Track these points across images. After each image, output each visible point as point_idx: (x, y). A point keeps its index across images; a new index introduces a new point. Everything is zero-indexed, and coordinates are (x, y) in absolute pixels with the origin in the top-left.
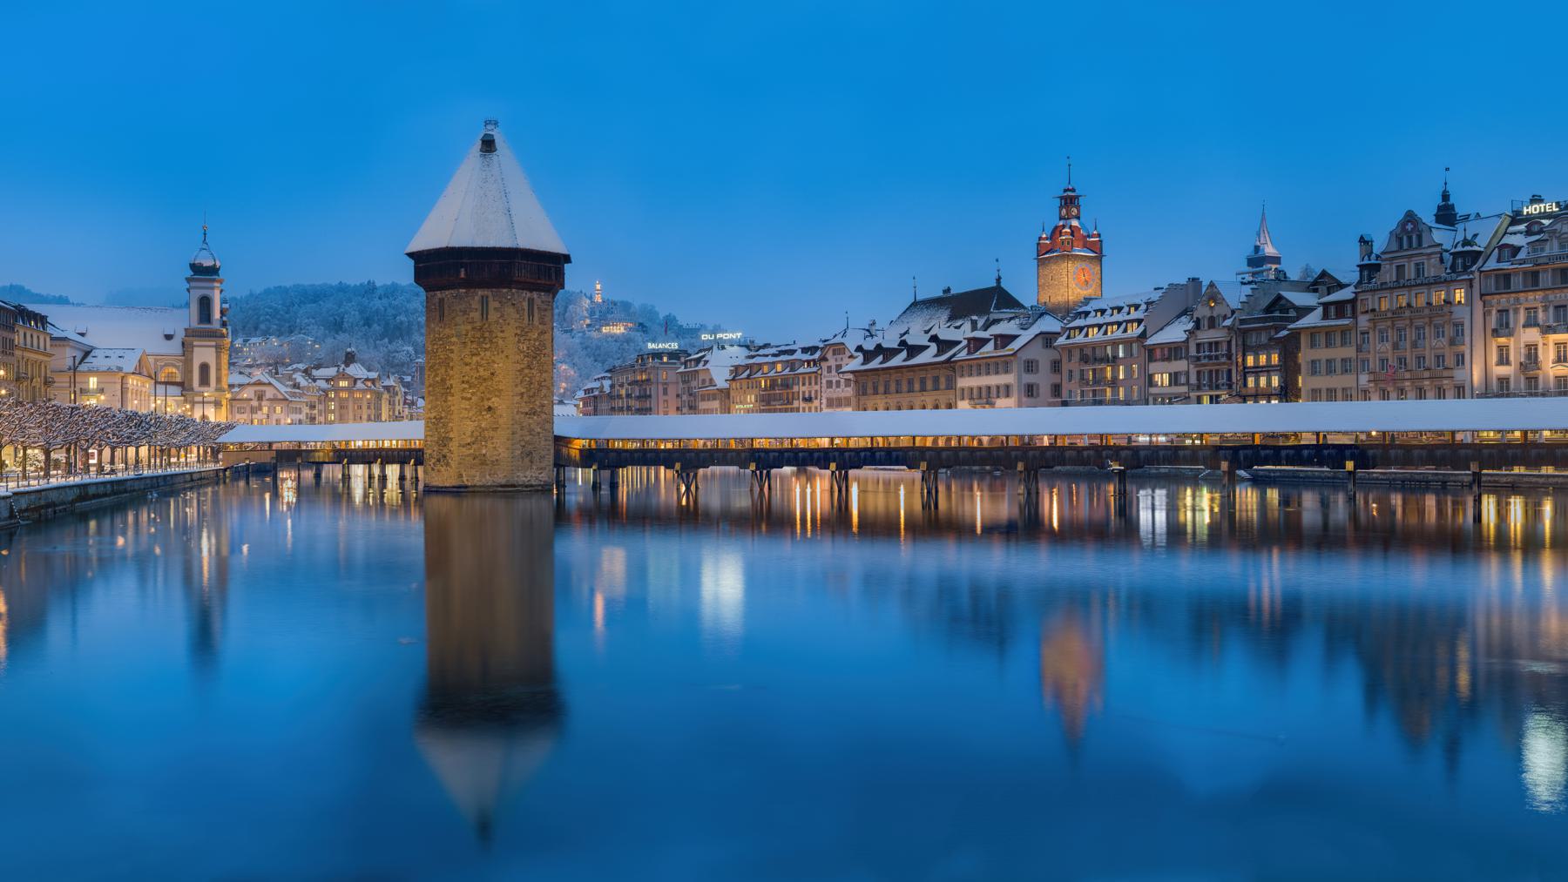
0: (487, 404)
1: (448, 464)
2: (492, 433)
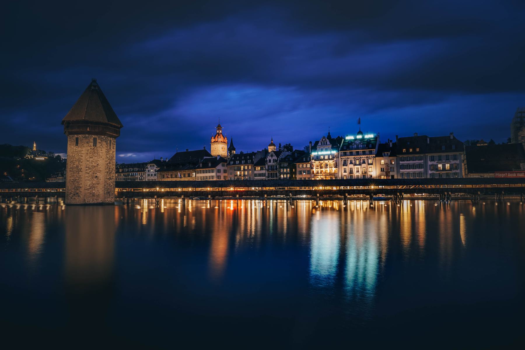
0: (95, 175)
1: (79, 196)
2: (97, 185)
